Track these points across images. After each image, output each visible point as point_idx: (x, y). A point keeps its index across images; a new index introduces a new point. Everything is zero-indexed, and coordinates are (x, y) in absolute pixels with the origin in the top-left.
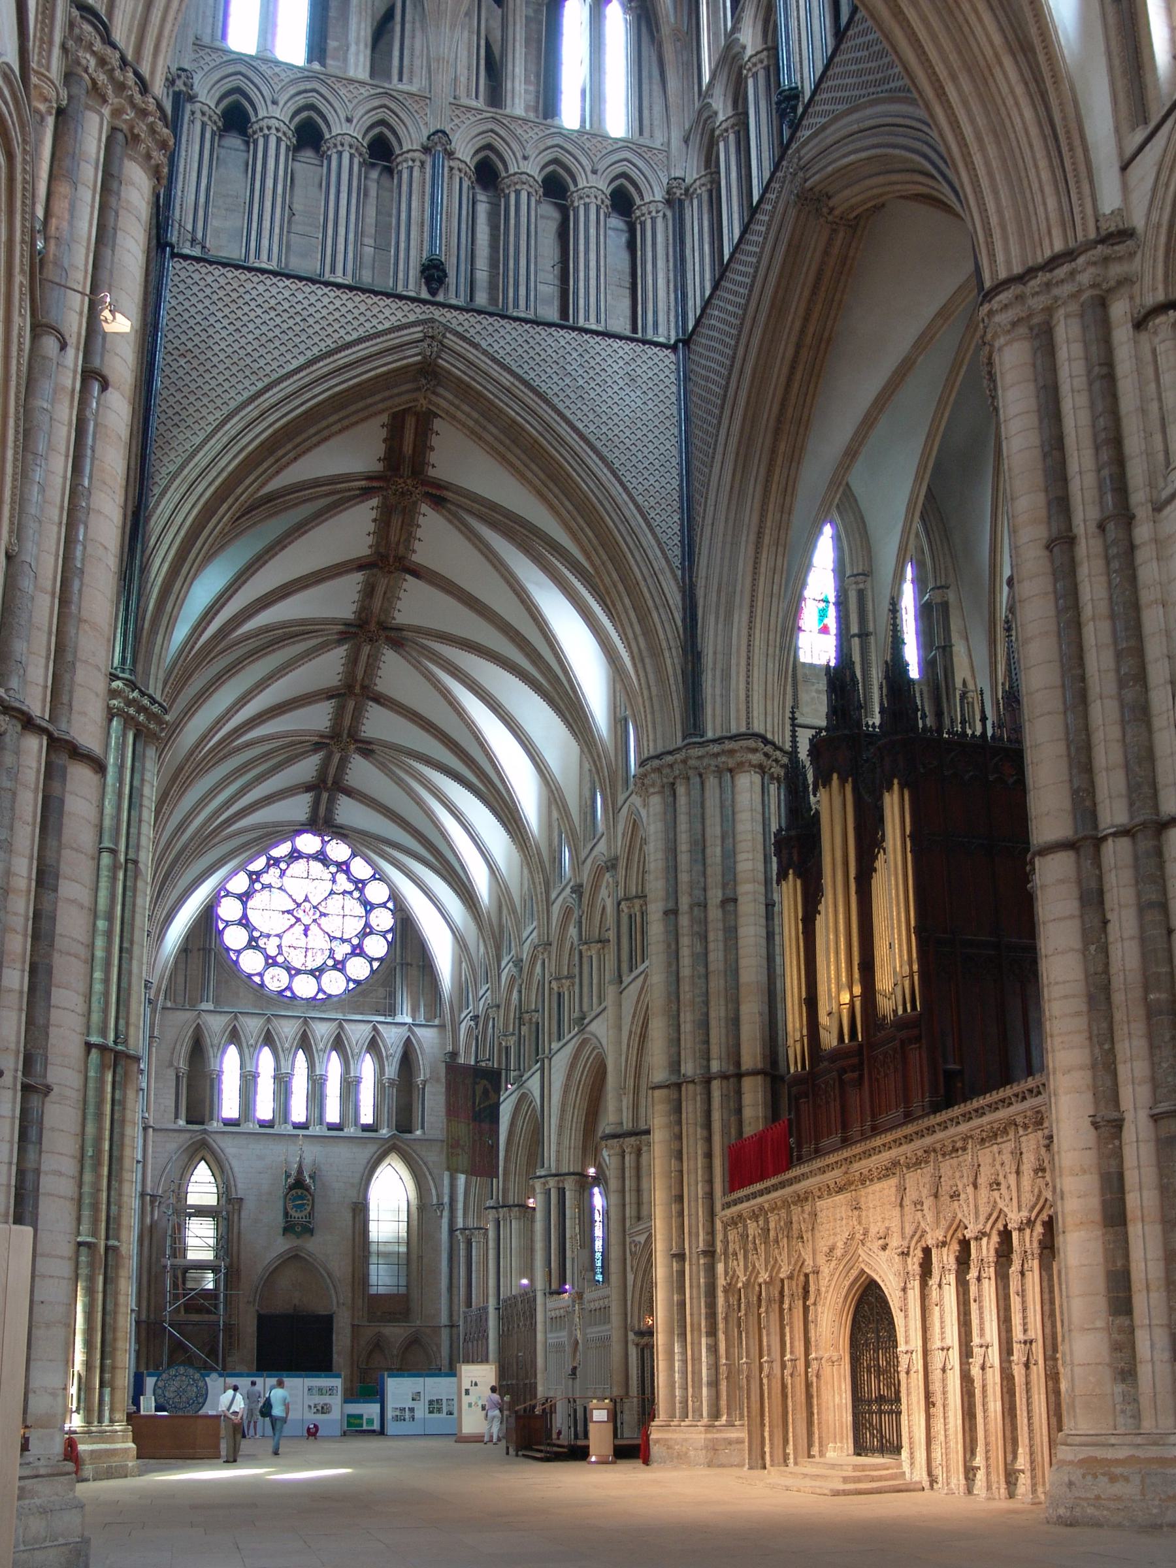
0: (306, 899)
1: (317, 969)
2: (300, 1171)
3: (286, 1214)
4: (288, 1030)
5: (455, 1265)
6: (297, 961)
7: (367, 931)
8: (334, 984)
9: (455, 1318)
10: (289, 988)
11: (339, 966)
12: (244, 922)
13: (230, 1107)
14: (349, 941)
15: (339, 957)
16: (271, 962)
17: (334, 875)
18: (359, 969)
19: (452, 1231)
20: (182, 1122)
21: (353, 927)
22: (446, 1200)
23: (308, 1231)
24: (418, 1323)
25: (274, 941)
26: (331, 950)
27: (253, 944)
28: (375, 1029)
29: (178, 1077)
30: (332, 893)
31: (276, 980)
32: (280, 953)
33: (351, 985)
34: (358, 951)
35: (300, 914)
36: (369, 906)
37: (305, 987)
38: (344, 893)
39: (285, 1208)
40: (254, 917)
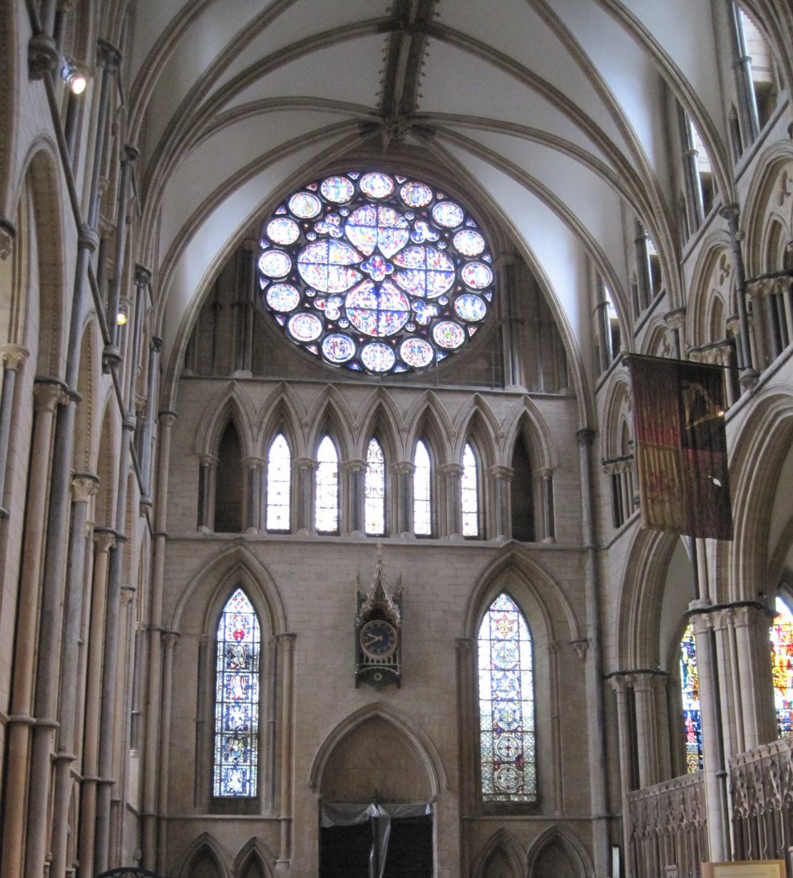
0: (377, 251)
1: (393, 336)
2: (379, 594)
3: (360, 657)
4: (356, 404)
5: (611, 729)
6: (366, 325)
7: (460, 289)
8: (418, 355)
10: (357, 359)
11: (424, 333)
12: (293, 279)
13: (278, 516)
14: (434, 302)
15: (423, 321)
16: (331, 328)
19: (603, 677)
20: (207, 530)
21: (440, 285)
22: (591, 634)
23: (391, 680)
25: (336, 303)
26: (411, 312)
27: (307, 306)
28: (478, 401)
29: (202, 469)
30: (410, 244)
31: (338, 351)
32: (343, 317)
33: (441, 357)
34: (447, 313)
35: (369, 269)
36: (459, 260)
37: (378, 359)
38: (427, 244)
39: (358, 647)
40: (309, 275)
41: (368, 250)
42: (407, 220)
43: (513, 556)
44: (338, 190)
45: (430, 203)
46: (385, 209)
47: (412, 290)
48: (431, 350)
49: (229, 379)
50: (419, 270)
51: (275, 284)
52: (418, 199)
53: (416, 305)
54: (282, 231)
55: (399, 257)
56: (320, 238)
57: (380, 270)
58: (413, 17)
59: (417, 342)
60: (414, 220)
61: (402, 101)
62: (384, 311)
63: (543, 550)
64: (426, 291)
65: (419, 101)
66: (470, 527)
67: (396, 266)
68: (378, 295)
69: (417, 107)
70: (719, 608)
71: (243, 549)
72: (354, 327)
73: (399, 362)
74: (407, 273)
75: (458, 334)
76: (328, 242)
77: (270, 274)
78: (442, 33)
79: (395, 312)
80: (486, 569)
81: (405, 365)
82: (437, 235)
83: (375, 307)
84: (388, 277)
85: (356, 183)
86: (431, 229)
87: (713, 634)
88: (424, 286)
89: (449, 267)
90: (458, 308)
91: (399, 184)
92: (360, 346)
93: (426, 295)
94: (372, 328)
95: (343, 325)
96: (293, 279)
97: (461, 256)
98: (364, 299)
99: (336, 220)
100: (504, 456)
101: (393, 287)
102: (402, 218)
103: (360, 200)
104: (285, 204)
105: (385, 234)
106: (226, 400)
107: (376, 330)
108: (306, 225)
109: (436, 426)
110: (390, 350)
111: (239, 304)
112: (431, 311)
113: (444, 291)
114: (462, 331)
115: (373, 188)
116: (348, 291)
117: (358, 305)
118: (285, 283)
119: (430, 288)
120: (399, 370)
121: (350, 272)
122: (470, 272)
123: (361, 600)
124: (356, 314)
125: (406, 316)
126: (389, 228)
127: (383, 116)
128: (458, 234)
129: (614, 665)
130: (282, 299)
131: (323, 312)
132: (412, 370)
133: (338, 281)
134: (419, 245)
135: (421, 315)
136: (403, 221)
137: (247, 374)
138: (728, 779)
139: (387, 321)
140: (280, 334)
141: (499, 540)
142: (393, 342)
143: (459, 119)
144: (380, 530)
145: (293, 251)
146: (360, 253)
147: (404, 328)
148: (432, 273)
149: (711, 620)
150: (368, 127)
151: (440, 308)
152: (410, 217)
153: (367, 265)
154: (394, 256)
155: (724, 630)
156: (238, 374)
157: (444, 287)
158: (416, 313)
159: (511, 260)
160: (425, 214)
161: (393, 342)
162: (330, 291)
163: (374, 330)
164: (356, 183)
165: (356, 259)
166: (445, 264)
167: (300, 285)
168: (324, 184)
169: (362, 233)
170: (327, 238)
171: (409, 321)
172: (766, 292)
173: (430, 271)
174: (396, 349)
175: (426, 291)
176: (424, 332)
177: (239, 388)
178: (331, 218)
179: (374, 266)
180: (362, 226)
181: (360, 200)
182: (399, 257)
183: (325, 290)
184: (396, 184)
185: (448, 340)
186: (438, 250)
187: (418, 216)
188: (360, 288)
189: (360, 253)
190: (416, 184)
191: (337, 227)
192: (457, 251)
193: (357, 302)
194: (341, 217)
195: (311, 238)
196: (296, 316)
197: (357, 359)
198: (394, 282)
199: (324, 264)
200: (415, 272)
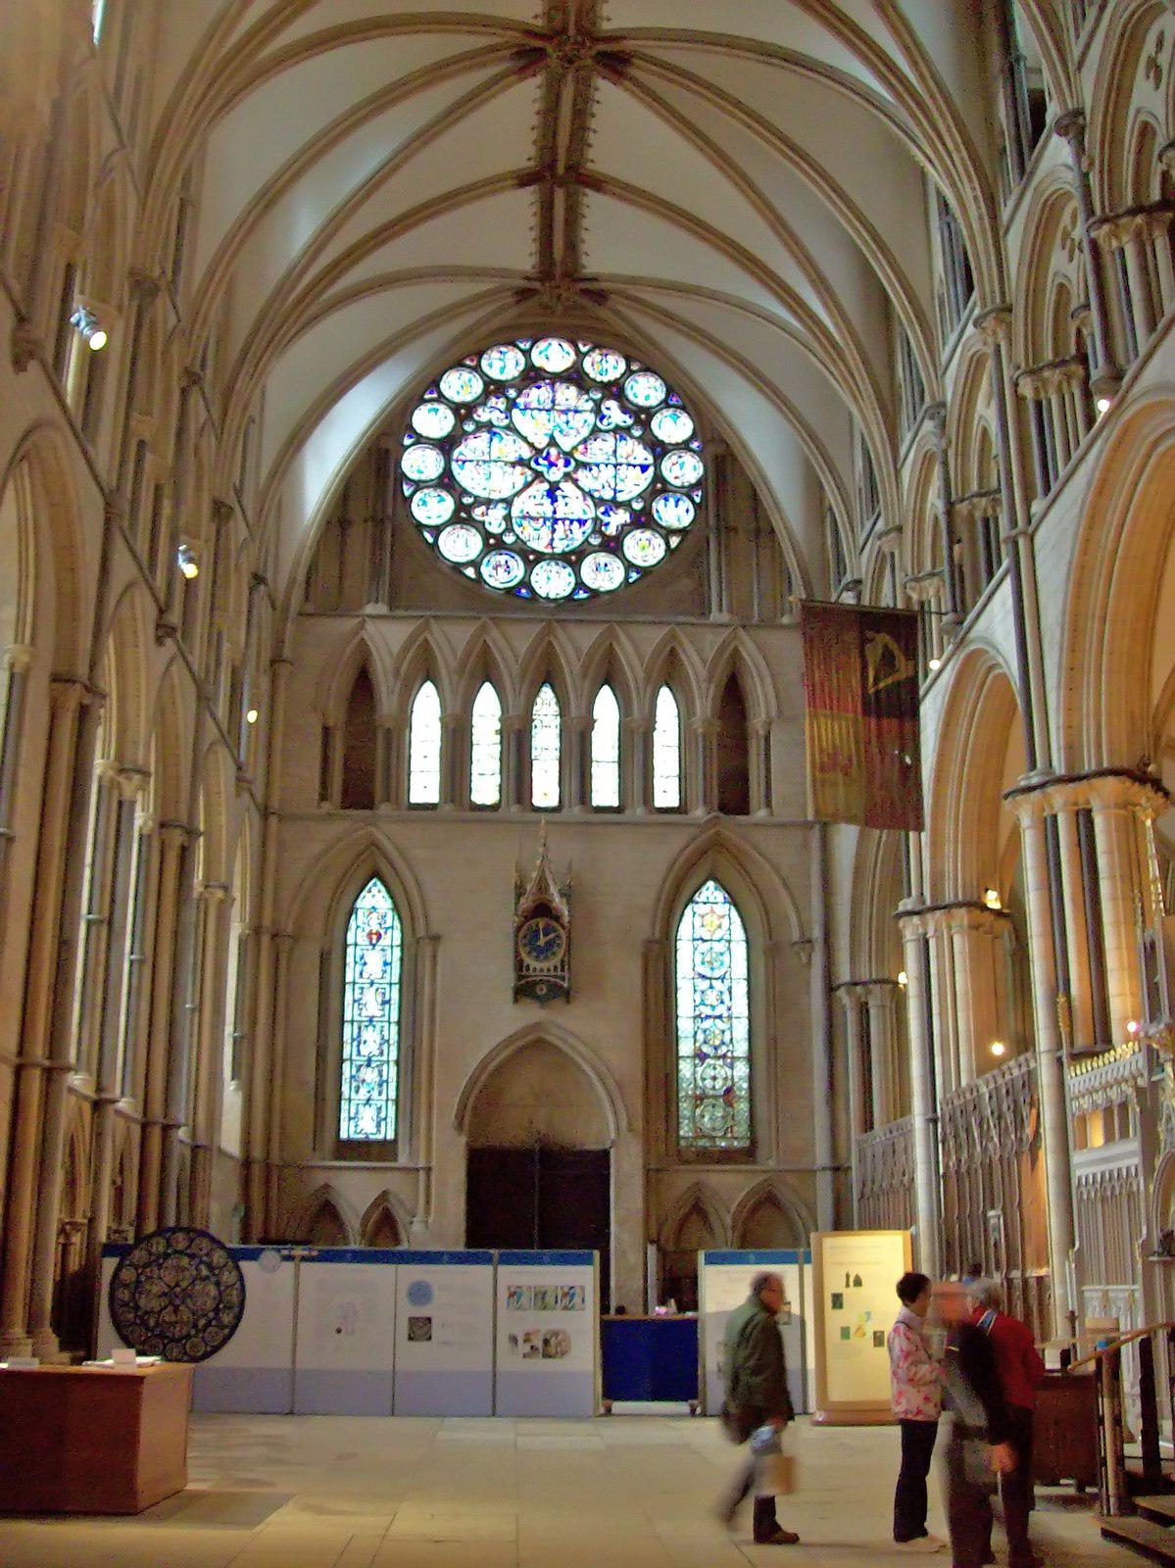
1: (572, 552)
2: (542, 886)
3: (520, 965)
4: (516, 642)
5: (839, 1054)
6: (537, 538)
7: (659, 488)
8: (604, 575)
9: (842, 1152)
10: (525, 583)
11: (613, 545)
12: (446, 481)
13: (425, 784)
14: (627, 505)
15: (611, 531)
16: (493, 544)
17: (598, 404)
18: (646, 549)
19: (830, 989)
21: (633, 484)
22: (817, 933)
23: (559, 993)
24: (772, 1164)
27: (462, 516)
29: (326, 730)
30: (595, 432)
31: (500, 574)
32: (509, 529)
33: (634, 576)
34: (643, 520)
36: (659, 449)
38: (621, 432)
39: (517, 954)
40: (465, 476)
41: (541, 442)
43: (718, 834)
44: (504, 364)
46: (564, 385)
49: (358, 616)
51: (423, 488)
54: (432, 421)
56: (481, 427)
58: (561, 169)
59: (603, 558)
61: (564, 261)
63: (756, 825)
65: (585, 260)
66: (666, 794)
68: (554, 500)
69: (584, 267)
70: (934, 909)
71: (374, 830)
73: (580, 585)
74: (591, 470)
77: (415, 476)
78: (598, 184)
80: (682, 851)
81: (587, 589)
83: (549, 514)
84: (567, 476)
85: (527, 353)
86: (625, 410)
87: (927, 942)
92: (530, 566)
93: (615, 497)
94: (547, 541)
95: (509, 539)
96: (446, 481)
97: (662, 443)
99: (501, 404)
100: (705, 705)
102: (586, 397)
103: (532, 376)
104: (435, 384)
105: (564, 418)
106: (356, 640)
108: (463, 412)
109: (622, 670)
110: (569, 570)
111: (373, 518)
112: (621, 517)
120: (582, 595)
121: (519, 469)
123: (520, 891)
125: (589, 524)
126: (569, 410)
127: (542, 280)
129: (844, 974)
130: (431, 508)
131: (483, 523)
132: (595, 594)
133: (503, 482)
134: (607, 432)
137: (381, 609)
138: (939, 1125)
140: (428, 551)
141: (699, 813)
142: (573, 559)
143: (634, 281)
144: (554, 802)
145: (446, 446)
146: (531, 445)
149: (924, 924)
150: (523, 294)
151: (633, 513)
152: (598, 396)
154: (575, 448)
155: (939, 938)
156: (370, 609)
158: (601, 521)
159: (720, 450)
161: (573, 559)
162: (492, 497)
164: (527, 353)
165: (526, 453)
166: (643, 455)
167: (455, 489)
168: (485, 356)
170: (489, 426)
171: (594, 531)
172: (978, 515)
174: (576, 567)
177: (371, 627)
181: (532, 376)
184: (578, 352)
186: (632, 437)
188: (531, 491)
189: (531, 445)
190: (604, 351)
195: (469, 427)
197: (525, 583)
198: (575, 482)
199: (485, 462)
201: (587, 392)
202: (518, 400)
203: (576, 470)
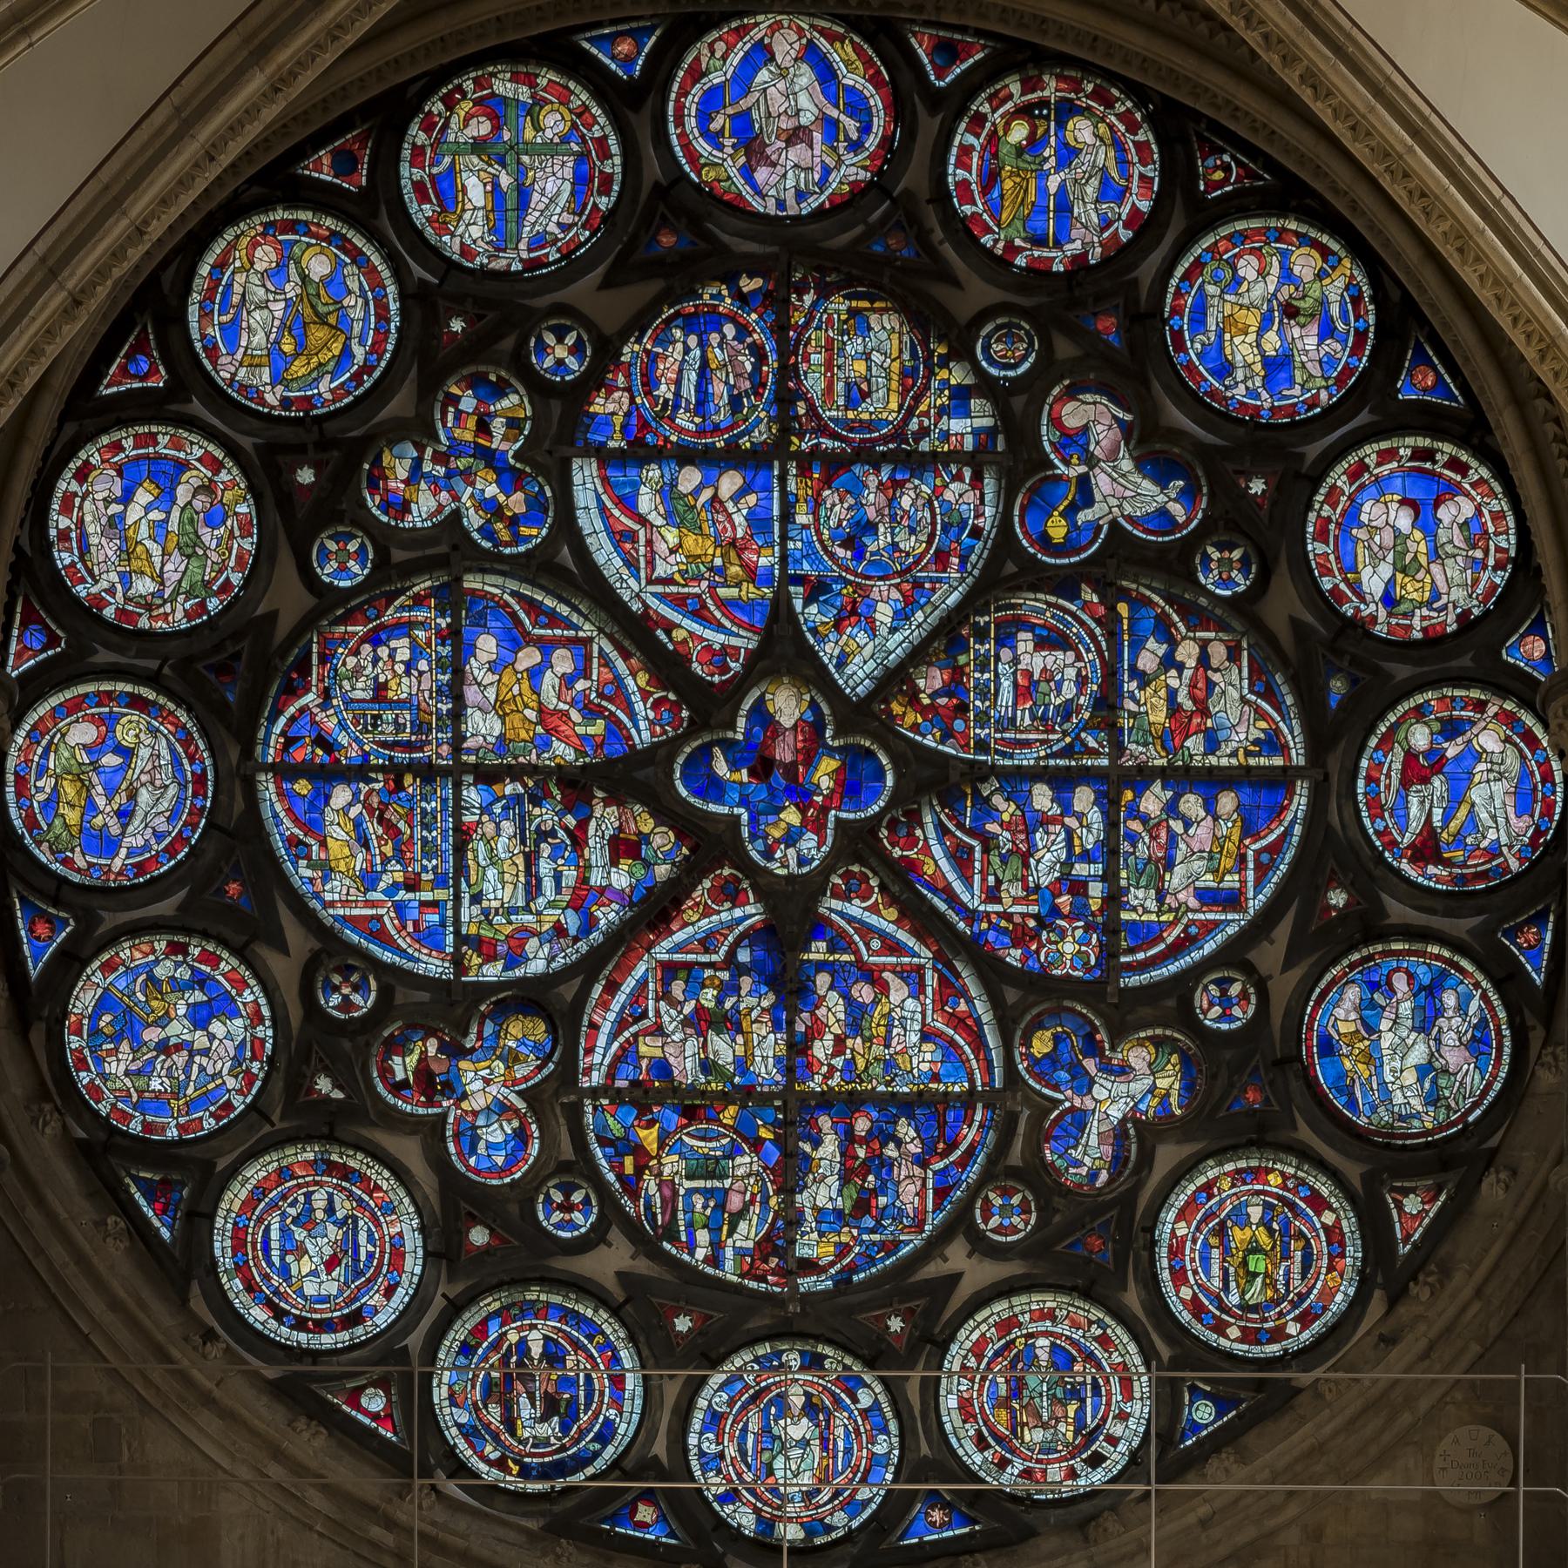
42: (985, 386)
45: (1146, 228)
46: (838, 305)
47: (1020, 937)
48: (1142, 1386)
50: (1062, 782)
51: (113, 939)
52: (1064, 207)
53: (1041, 1045)
55: (931, 680)
57: (801, 795)
60: (1035, 385)
62: (826, 1101)
64: (1109, 928)
67: (909, 757)
72: (632, 1229)
75: (1320, 1246)
76: (450, 597)
79: (907, 1105)
82: (1189, 496)
88: (1096, 890)
89: (1272, 743)
90: (1328, 1047)
91: (936, 99)
94: (747, 1234)
98: (702, 1022)
101: (886, 921)
102: (958, 375)
107: (777, 1243)
113: (1234, 922)
114: (1348, 1225)
115: (752, 146)
116: (589, 967)
117: (662, 1067)
118: (179, 928)
119: (1140, 903)
121: (605, 819)
122: (1417, 771)
124: (649, 1137)
128: (1338, 477)
134: (1065, 584)
135: (1080, 1119)
136: (961, 395)
139: (845, 1178)
147: (960, 1224)
148: (1152, 802)
153: (721, 768)
154: (895, 680)
157: (1233, 901)
160: (1108, 326)
163: (766, 1246)
169: (677, 509)
173: (1142, 777)
175: (1109, 953)
176: (1097, 1246)
178: (468, 403)
179: (763, 767)
180: (685, 456)
182: (931, 680)
183: (433, 966)
185: (1255, 1293)
186: (1197, 617)
187: (1064, 348)
191: (511, 479)
192: (1326, 605)
193: (649, 1048)
194: (538, 387)
196: (255, 1173)
199: (428, 773)
200: (1042, 797)
201: (961, 352)
202: (600, 406)
203: (905, 814)
